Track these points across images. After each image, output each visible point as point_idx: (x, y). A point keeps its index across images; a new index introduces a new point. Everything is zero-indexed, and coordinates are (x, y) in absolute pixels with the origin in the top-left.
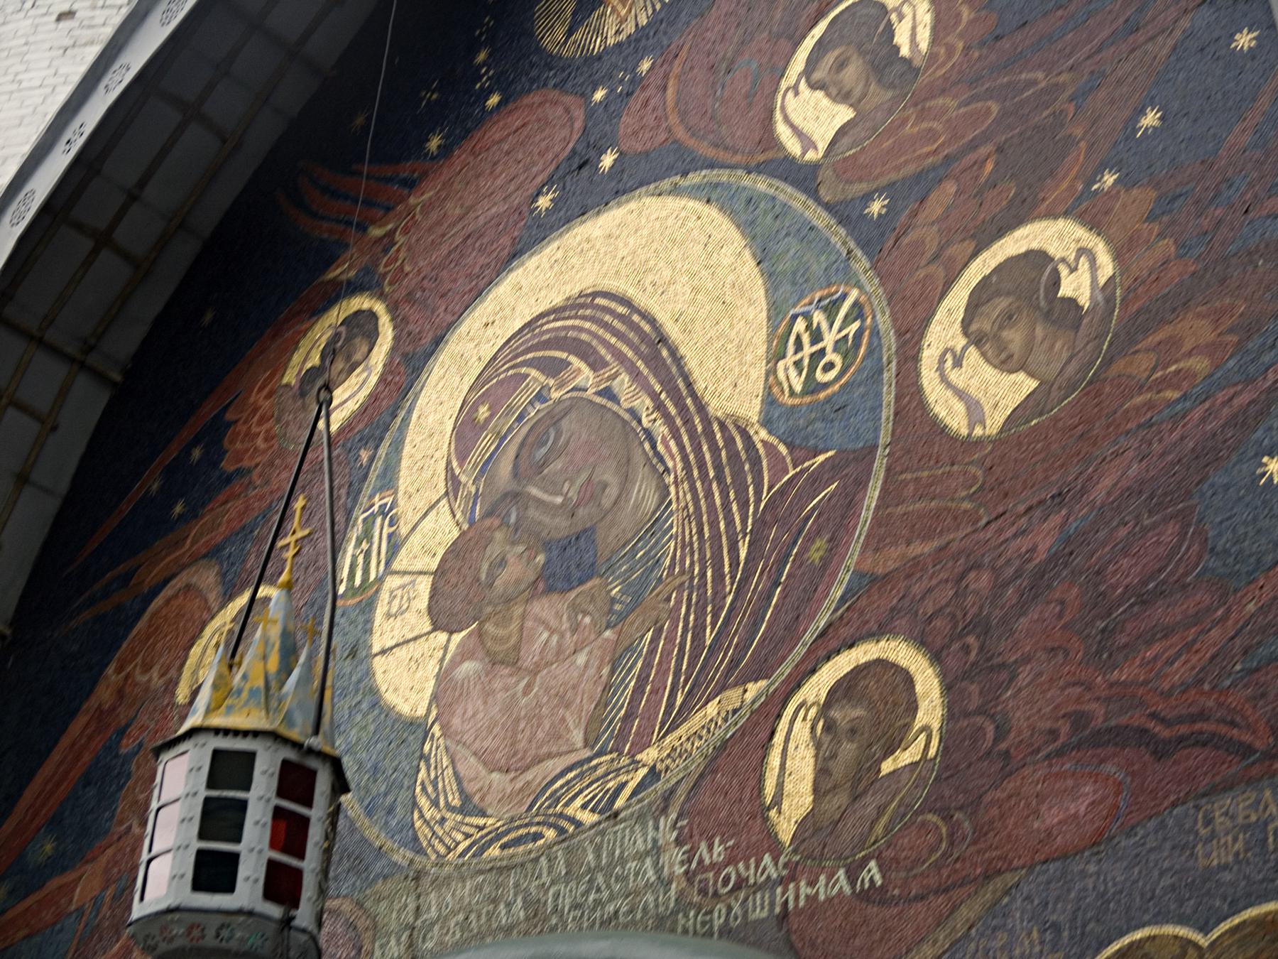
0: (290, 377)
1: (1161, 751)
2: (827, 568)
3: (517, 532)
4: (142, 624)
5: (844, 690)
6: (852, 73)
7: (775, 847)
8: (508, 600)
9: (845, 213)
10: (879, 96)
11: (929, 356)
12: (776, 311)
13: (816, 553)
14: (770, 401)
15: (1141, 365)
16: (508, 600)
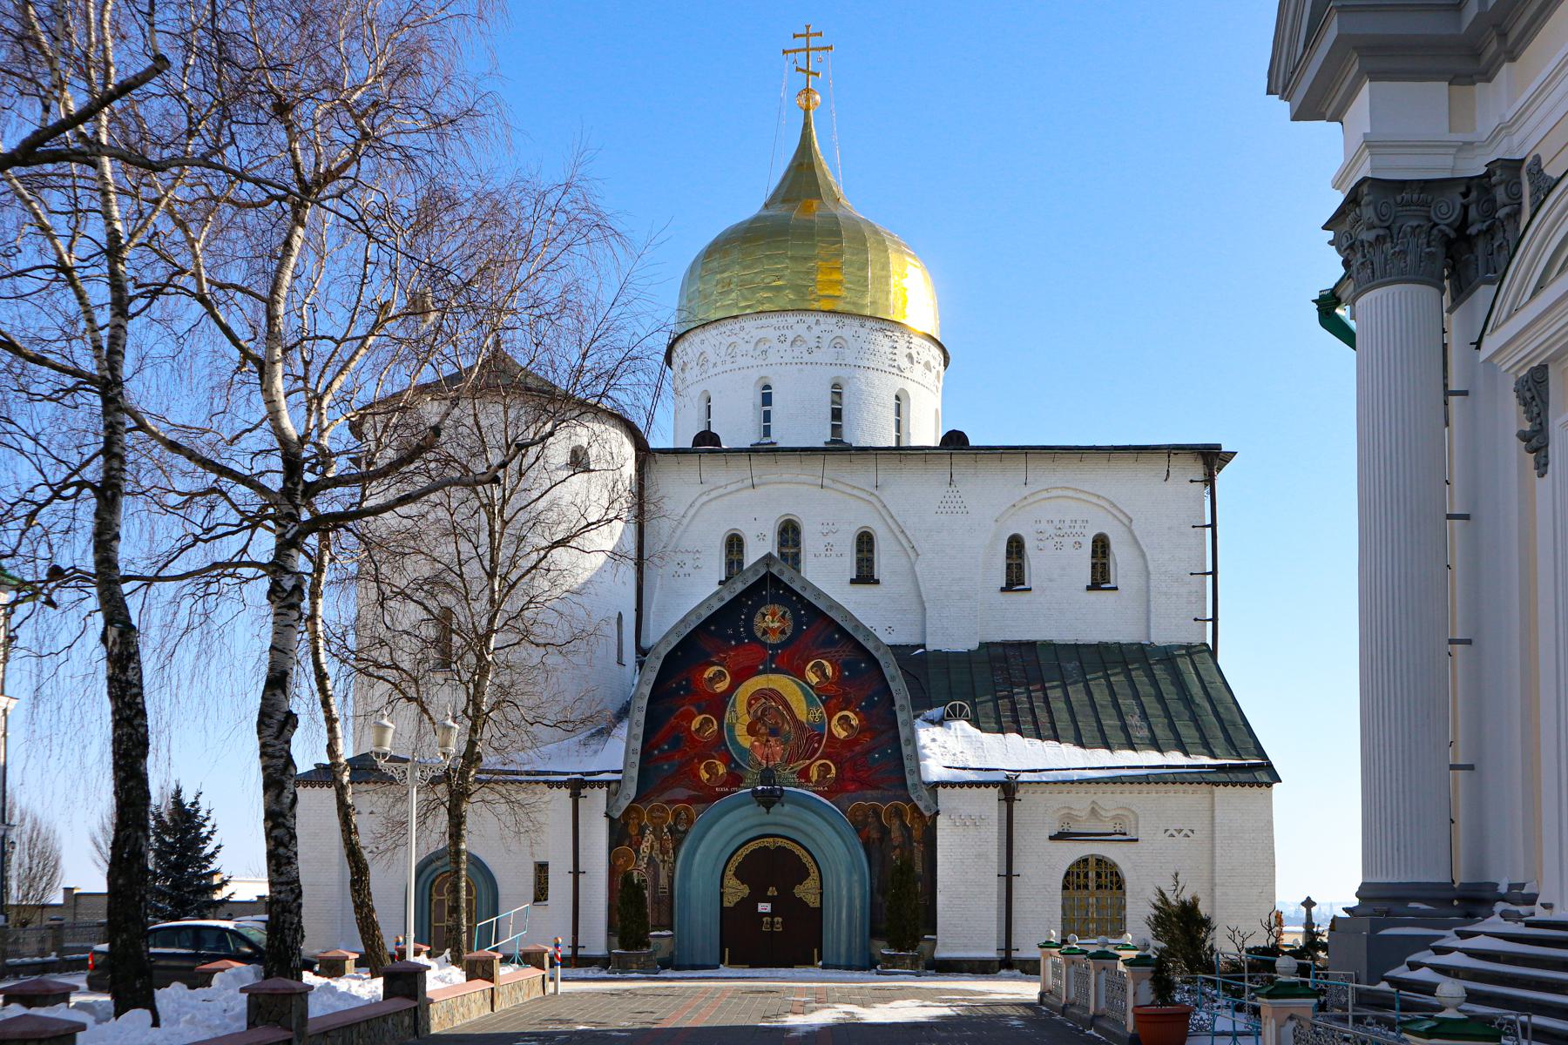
0: (705, 676)
1: (862, 784)
2: (818, 748)
3: (764, 724)
4: (678, 713)
5: (821, 765)
6: (819, 673)
7: (811, 781)
8: (763, 735)
9: (820, 699)
10: (823, 679)
11: (832, 724)
12: (807, 706)
13: (816, 745)
14: (808, 720)
15: (861, 737)
16: (763, 735)
